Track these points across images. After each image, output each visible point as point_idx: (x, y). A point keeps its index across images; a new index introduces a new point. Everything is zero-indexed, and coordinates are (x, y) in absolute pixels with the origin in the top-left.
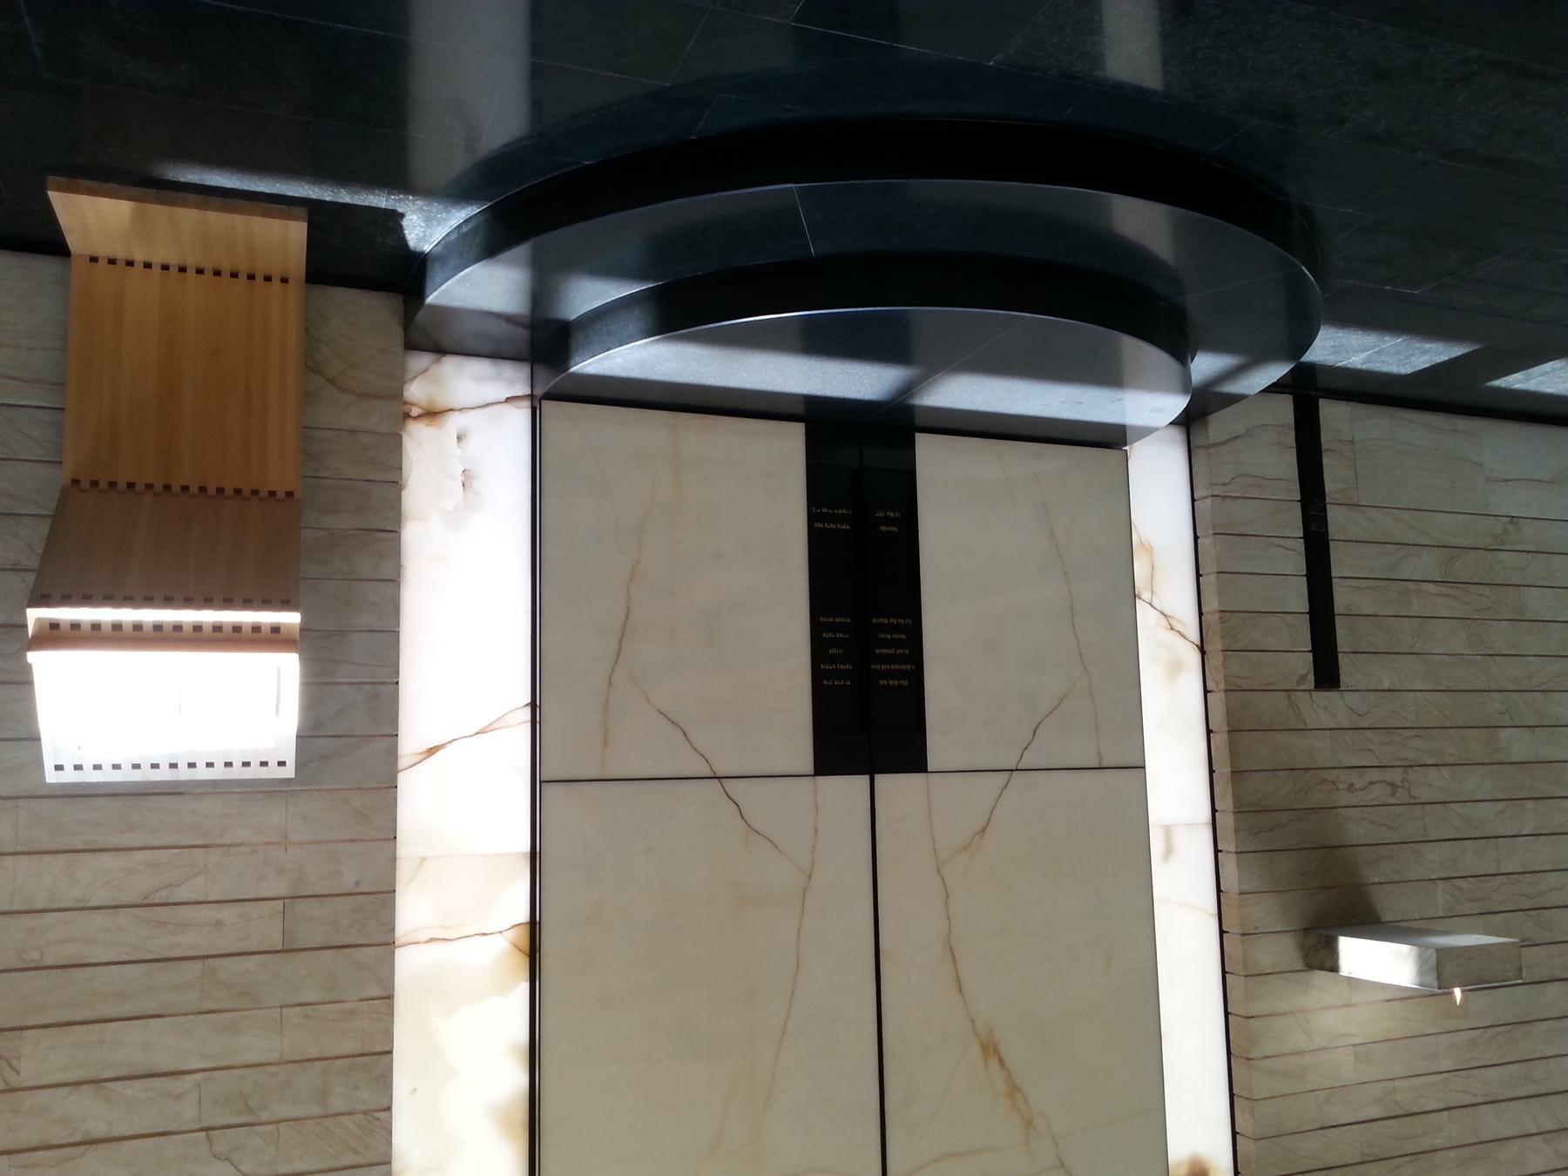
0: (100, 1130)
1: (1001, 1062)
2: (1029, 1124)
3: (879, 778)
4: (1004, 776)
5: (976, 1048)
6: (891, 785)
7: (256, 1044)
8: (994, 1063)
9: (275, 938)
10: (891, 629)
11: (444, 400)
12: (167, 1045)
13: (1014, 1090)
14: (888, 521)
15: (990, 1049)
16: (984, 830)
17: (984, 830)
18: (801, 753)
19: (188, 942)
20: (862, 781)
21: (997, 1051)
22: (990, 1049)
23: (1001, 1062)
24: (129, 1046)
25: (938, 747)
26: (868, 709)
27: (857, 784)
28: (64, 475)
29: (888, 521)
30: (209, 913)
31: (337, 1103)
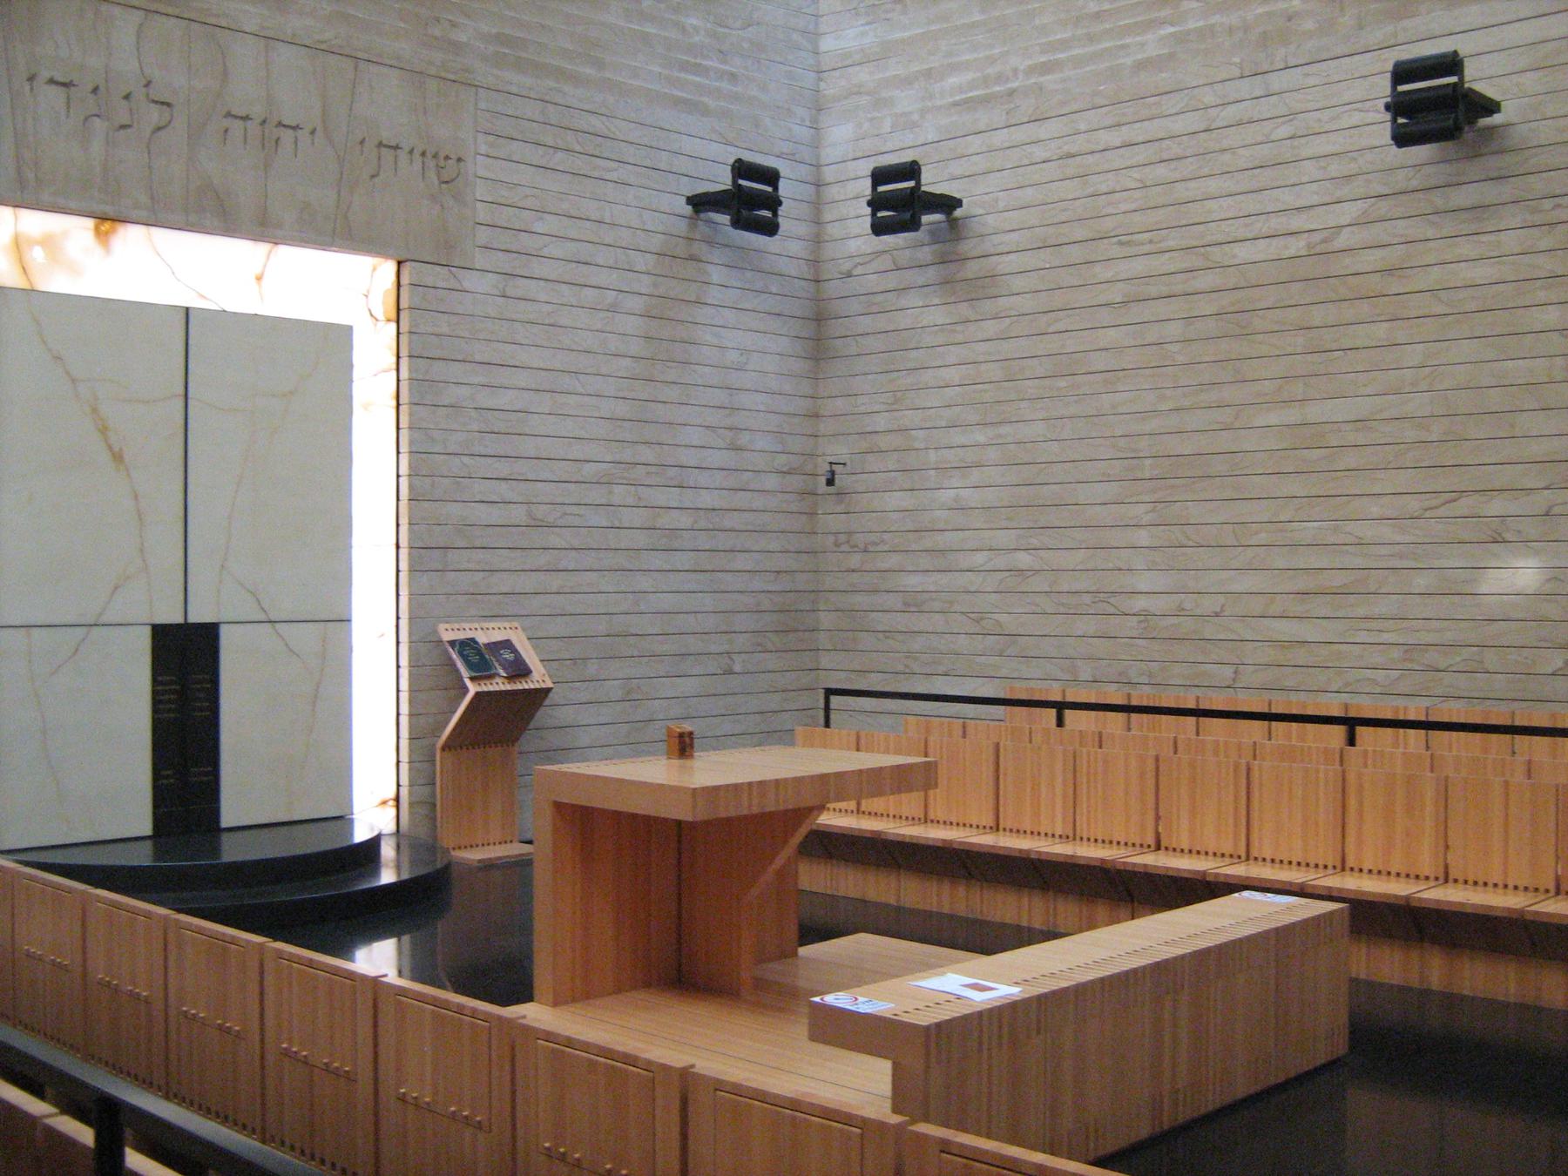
0: (503, 483)
1: (110, 448)
2: (95, 410)
3: (179, 620)
4: (105, 619)
5: (127, 458)
6: (174, 617)
7: (455, 510)
8: (116, 450)
9: (450, 553)
10: (169, 711)
11: (379, 809)
12: (483, 514)
13: (104, 431)
14: (167, 777)
15: (118, 457)
16: (116, 588)
17: (116, 588)
18: (225, 634)
19: (480, 554)
20: (192, 619)
21: (113, 454)
22: (118, 457)
23: (110, 448)
24: (495, 515)
25: (143, 642)
26: (186, 661)
27: (200, 614)
28: (516, 748)
29: (167, 777)
30: (471, 566)
31: (427, 480)
